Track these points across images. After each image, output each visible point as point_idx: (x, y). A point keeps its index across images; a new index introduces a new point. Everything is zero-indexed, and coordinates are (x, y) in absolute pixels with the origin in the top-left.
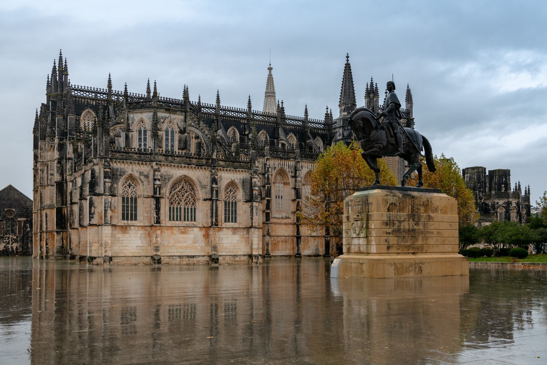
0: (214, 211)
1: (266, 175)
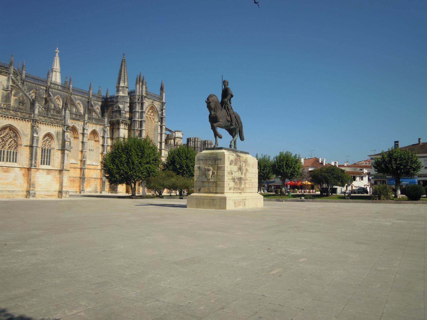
0: (34, 155)
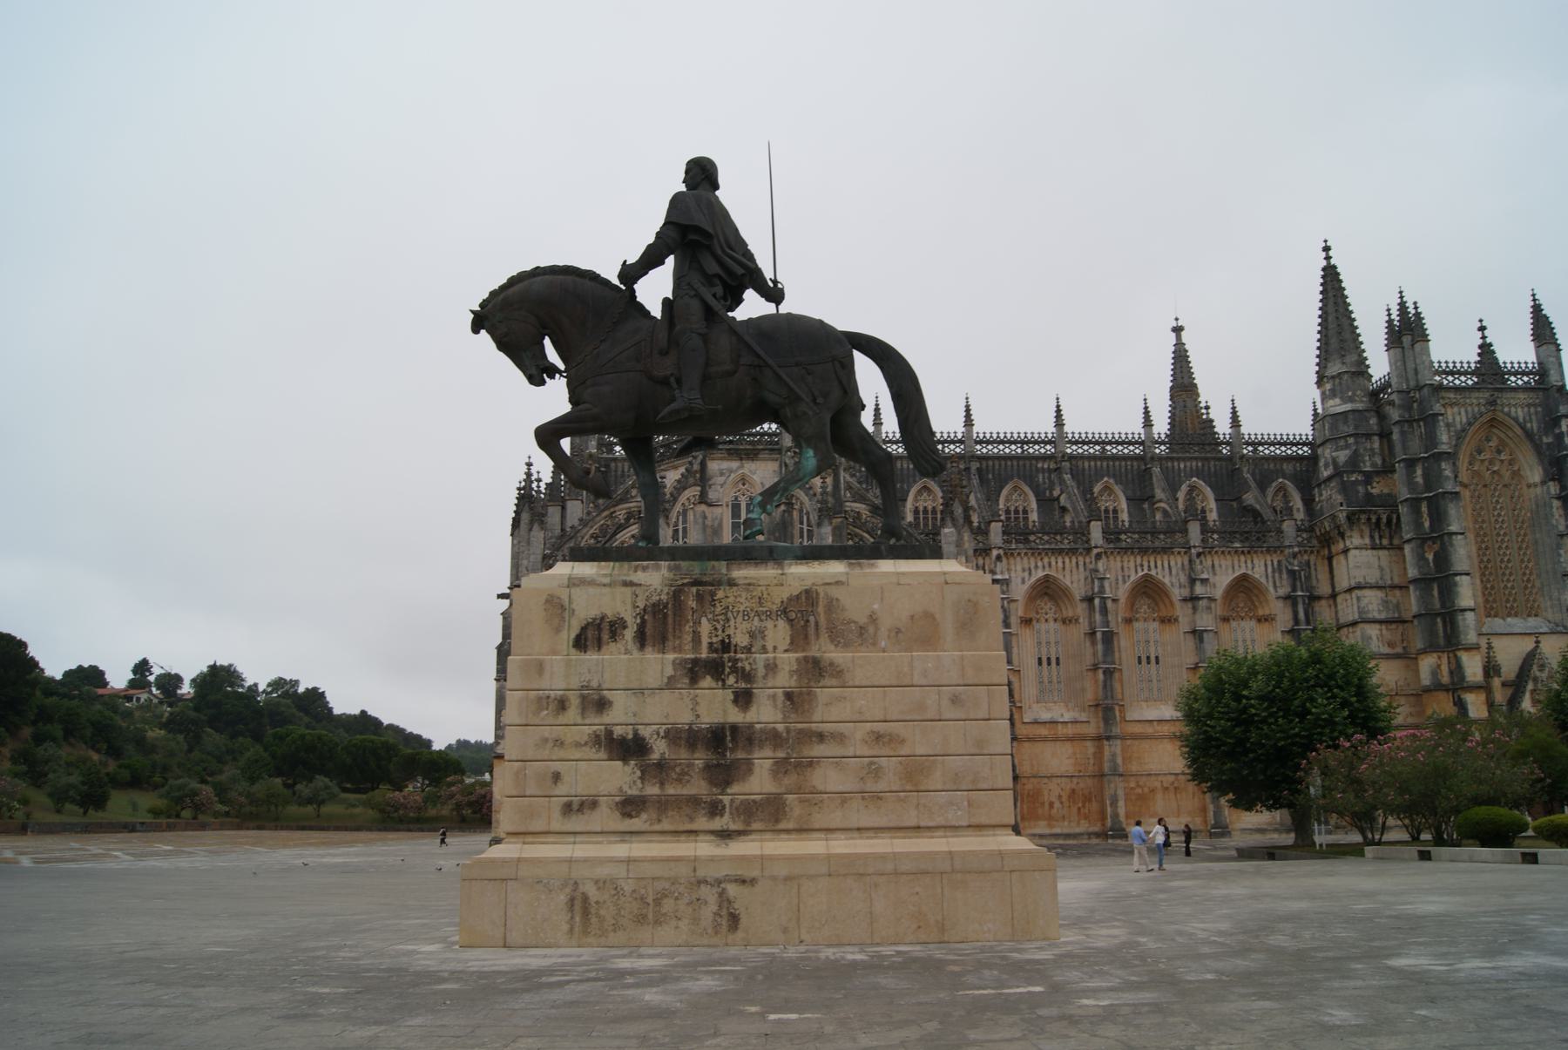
1: (1097, 601)
